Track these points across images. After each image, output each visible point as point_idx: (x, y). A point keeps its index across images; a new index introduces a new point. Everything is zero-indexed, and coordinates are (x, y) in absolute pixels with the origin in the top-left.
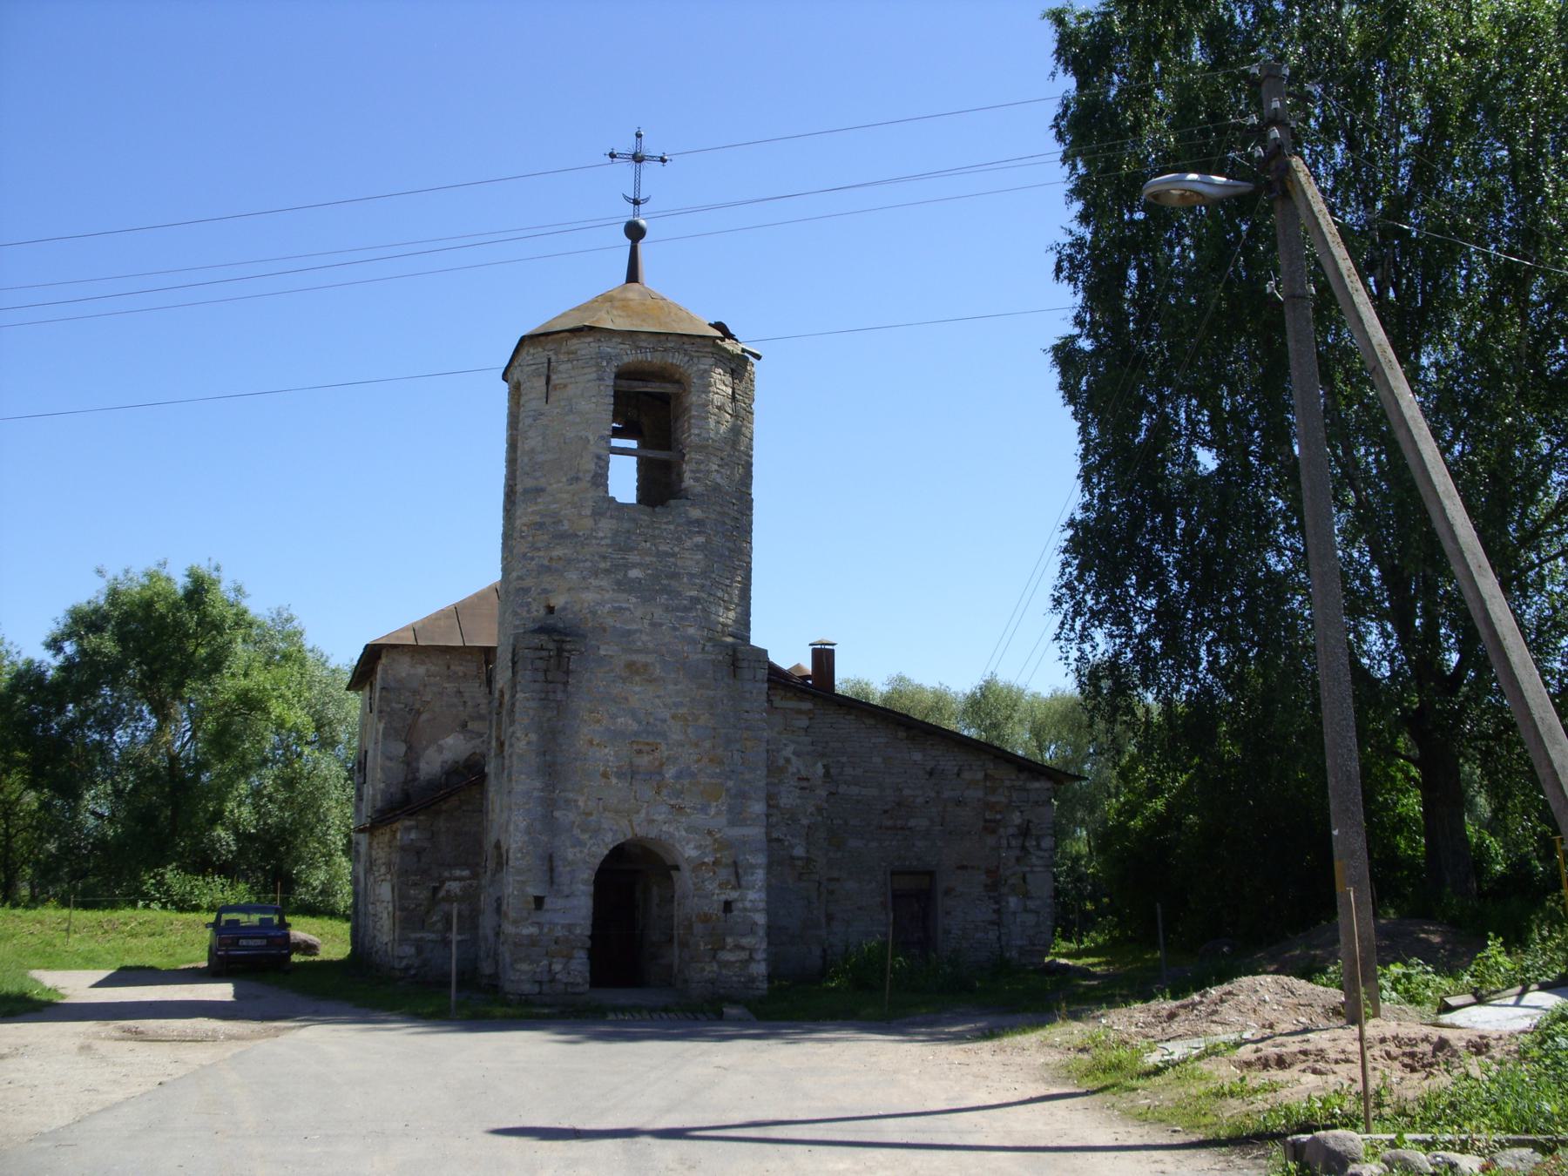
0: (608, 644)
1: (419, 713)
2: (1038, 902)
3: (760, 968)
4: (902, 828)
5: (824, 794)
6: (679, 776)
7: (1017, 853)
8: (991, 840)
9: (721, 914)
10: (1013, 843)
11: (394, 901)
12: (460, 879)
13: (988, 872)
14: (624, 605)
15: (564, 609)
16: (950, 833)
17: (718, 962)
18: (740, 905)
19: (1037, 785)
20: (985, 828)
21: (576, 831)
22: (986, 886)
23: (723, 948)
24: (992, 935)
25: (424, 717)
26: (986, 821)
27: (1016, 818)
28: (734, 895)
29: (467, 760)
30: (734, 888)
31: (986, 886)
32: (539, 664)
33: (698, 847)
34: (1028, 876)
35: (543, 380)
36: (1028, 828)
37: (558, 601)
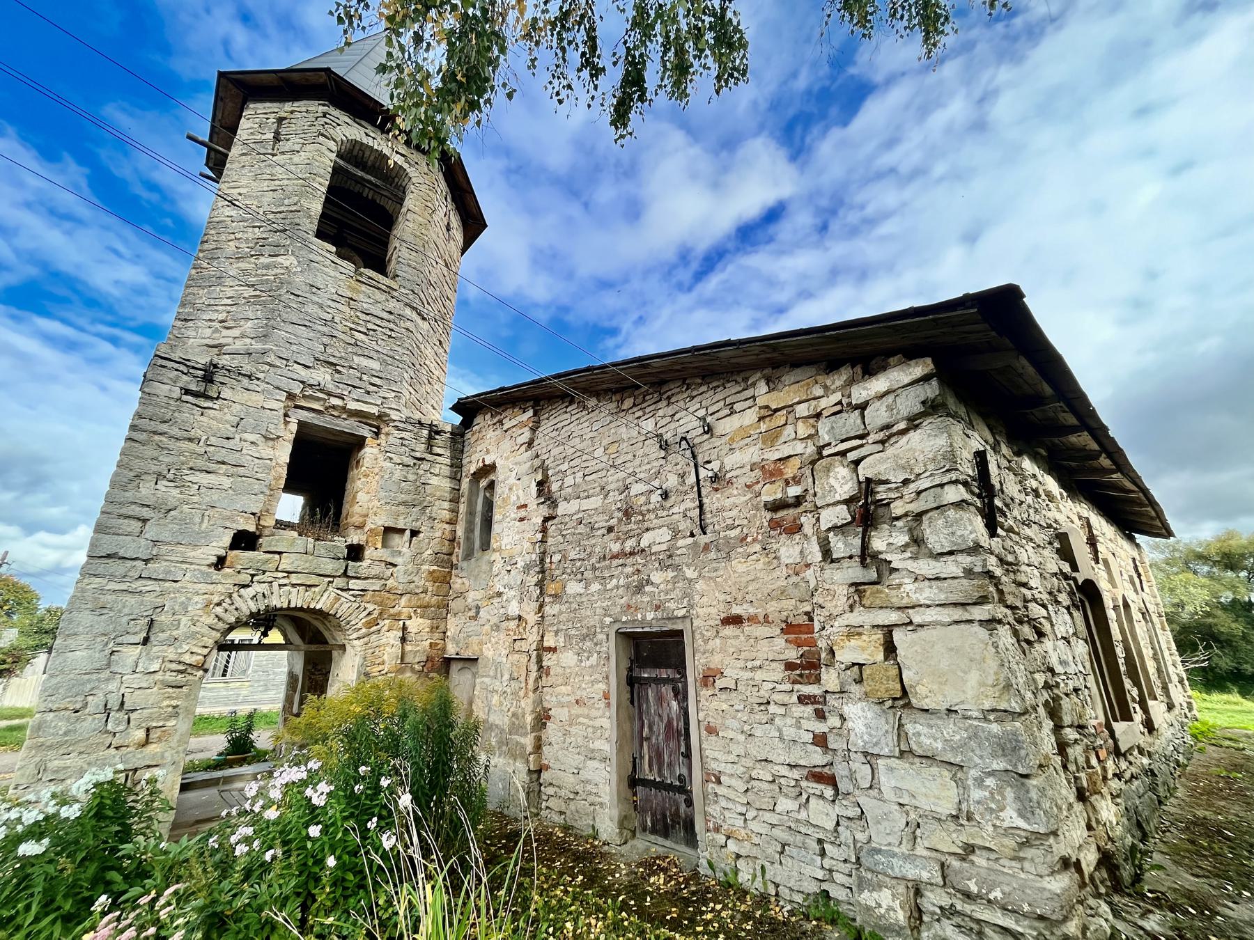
2: (952, 730)
4: (632, 554)
5: (540, 520)
7: (855, 572)
8: (788, 550)
10: (839, 546)
13: (789, 628)
19: (879, 384)
20: (774, 524)
22: (790, 666)
27: (841, 482)
31: (790, 666)
34: (898, 636)
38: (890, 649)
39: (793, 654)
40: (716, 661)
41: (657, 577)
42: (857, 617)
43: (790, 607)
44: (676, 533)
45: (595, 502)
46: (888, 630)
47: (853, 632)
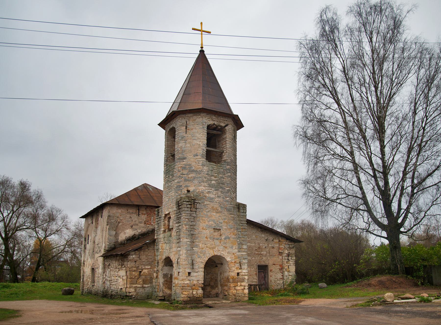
0: (207, 201)
1: (119, 223)
2: (292, 273)
3: (246, 291)
6: (225, 239)
7: (287, 260)
8: (281, 257)
9: (236, 276)
11: (126, 275)
12: (148, 269)
13: (280, 265)
14: (211, 191)
15: (194, 191)
16: (271, 255)
17: (236, 290)
18: (241, 274)
21: (199, 254)
22: (279, 269)
23: (237, 286)
24: (281, 282)
25: (120, 224)
26: (279, 252)
27: (286, 252)
28: (240, 271)
29: (132, 236)
30: (240, 269)
31: (279, 269)
32: (189, 206)
33: (230, 258)
35: (185, 127)
36: (289, 254)
37: (191, 189)
38: (288, 267)
39: (280, 268)
40: (272, 269)
41: (264, 258)
42: (287, 265)
43: (281, 263)
44: (267, 253)
45: (254, 245)
46: (288, 266)
47: (286, 266)
